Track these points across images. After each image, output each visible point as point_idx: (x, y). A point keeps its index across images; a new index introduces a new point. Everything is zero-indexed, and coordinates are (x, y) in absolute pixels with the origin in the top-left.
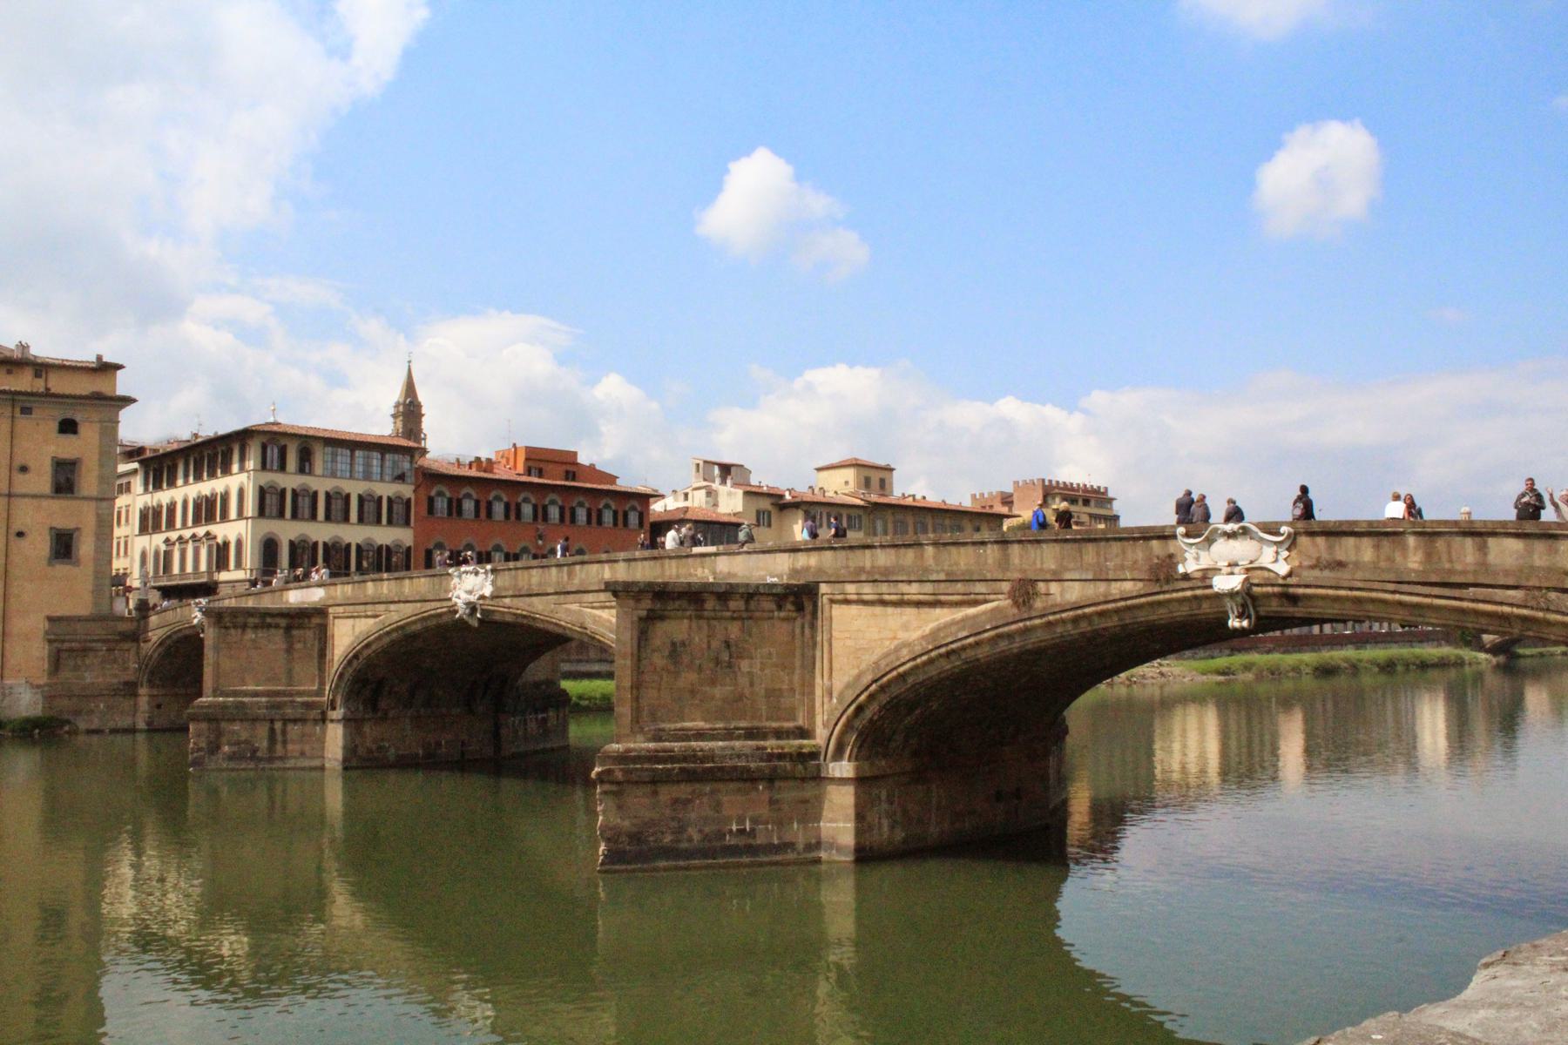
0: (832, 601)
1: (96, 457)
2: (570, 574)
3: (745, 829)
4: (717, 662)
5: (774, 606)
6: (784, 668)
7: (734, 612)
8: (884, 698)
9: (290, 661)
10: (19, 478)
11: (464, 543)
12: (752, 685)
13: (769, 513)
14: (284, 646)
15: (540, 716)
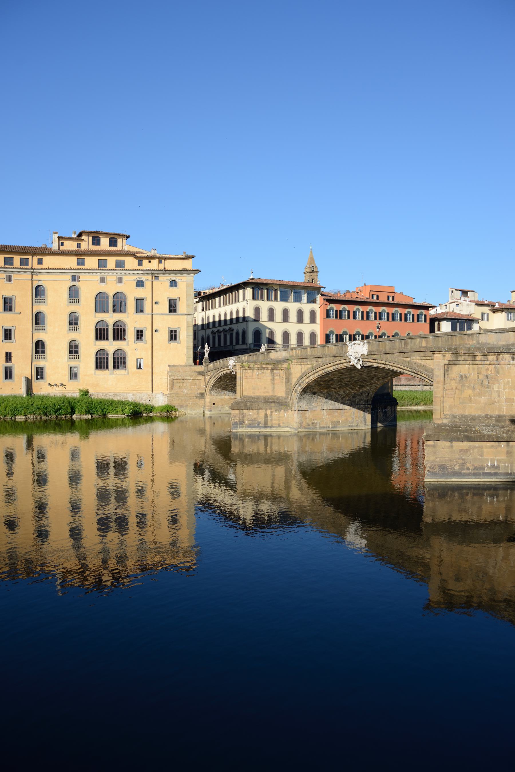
1: (185, 296)
2: (405, 344)
3: (495, 465)
5: (510, 359)
9: (273, 384)
10: (155, 306)
11: (342, 331)
12: (499, 396)
13: (488, 314)
14: (271, 378)
15: (384, 410)
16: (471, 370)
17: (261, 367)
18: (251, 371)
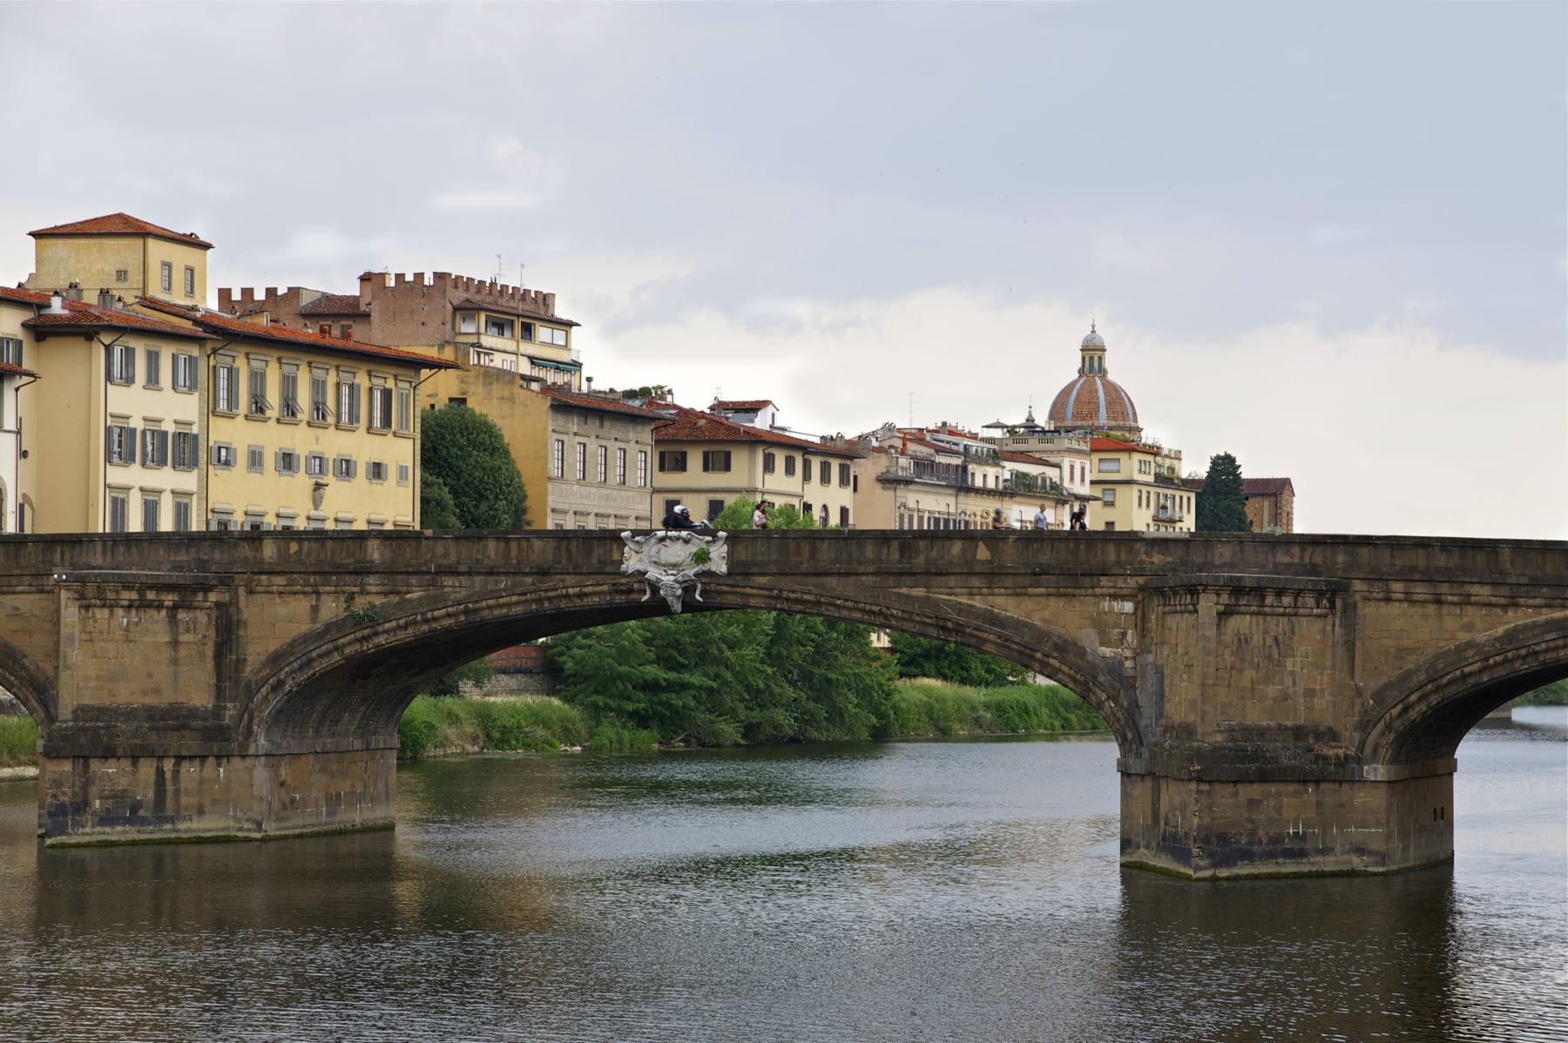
0: (1365, 599)
4: (1269, 657)
6: (1318, 667)
7: (1285, 608)
8: (1434, 700)
9: (175, 662)
16: (1254, 627)
17: (142, 598)
18: (106, 611)
